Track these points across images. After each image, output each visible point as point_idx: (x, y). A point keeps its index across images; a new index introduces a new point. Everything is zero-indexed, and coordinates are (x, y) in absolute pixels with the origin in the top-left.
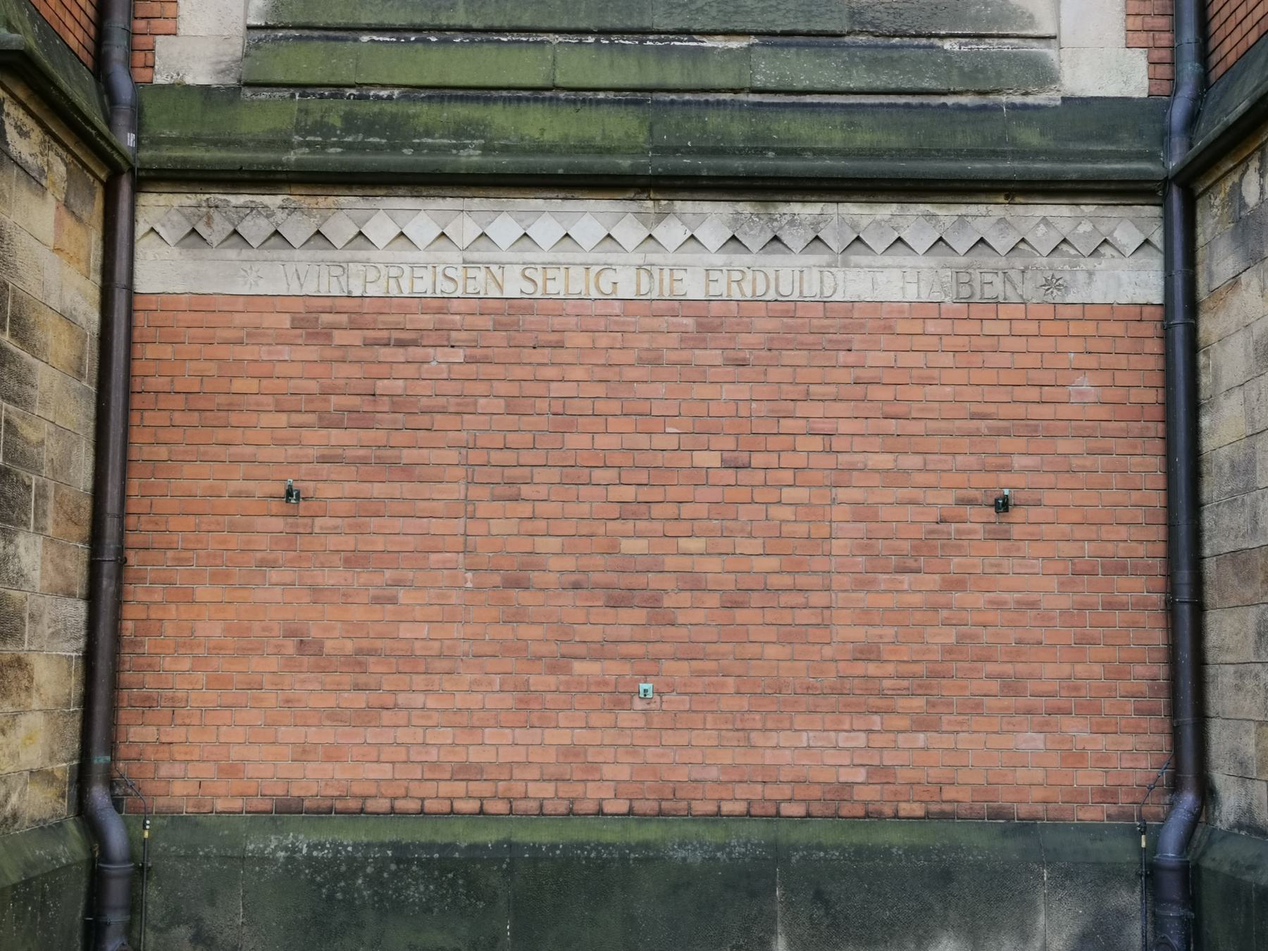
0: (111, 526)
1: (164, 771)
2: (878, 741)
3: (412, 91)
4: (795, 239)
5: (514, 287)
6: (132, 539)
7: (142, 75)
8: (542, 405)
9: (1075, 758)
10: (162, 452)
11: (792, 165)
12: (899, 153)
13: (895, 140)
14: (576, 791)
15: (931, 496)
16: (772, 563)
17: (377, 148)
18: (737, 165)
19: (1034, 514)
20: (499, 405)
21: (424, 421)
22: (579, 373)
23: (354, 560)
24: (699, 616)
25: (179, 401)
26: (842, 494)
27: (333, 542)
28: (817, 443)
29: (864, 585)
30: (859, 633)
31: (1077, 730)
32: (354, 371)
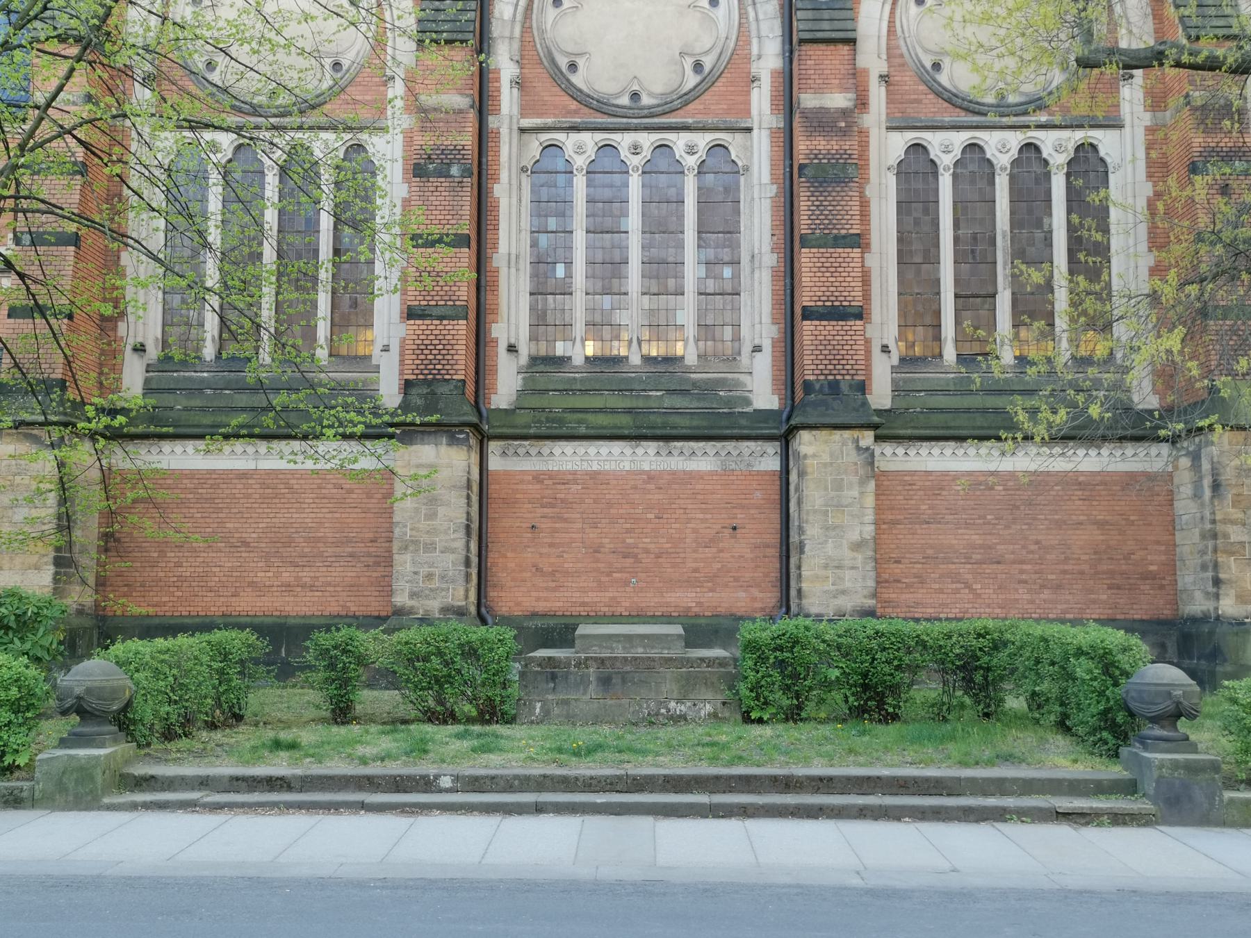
0: (484, 536)
1: (500, 604)
2: (699, 595)
3: (565, 410)
4: (675, 452)
5: (595, 467)
6: (489, 540)
7: (487, 406)
8: (604, 501)
9: (754, 599)
10: (497, 515)
11: (674, 432)
12: (705, 428)
13: (705, 423)
14: (614, 609)
15: (714, 526)
16: (670, 545)
17: (556, 428)
18: (658, 432)
19: (743, 531)
20: (592, 501)
21: (570, 505)
22: (614, 492)
23: (551, 545)
24: (649, 560)
25: (501, 501)
26: (689, 525)
27: (545, 540)
28: (682, 511)
29: (695, 551)
30: (694, 565)
31: (755, 592)
32: (550, 492)
